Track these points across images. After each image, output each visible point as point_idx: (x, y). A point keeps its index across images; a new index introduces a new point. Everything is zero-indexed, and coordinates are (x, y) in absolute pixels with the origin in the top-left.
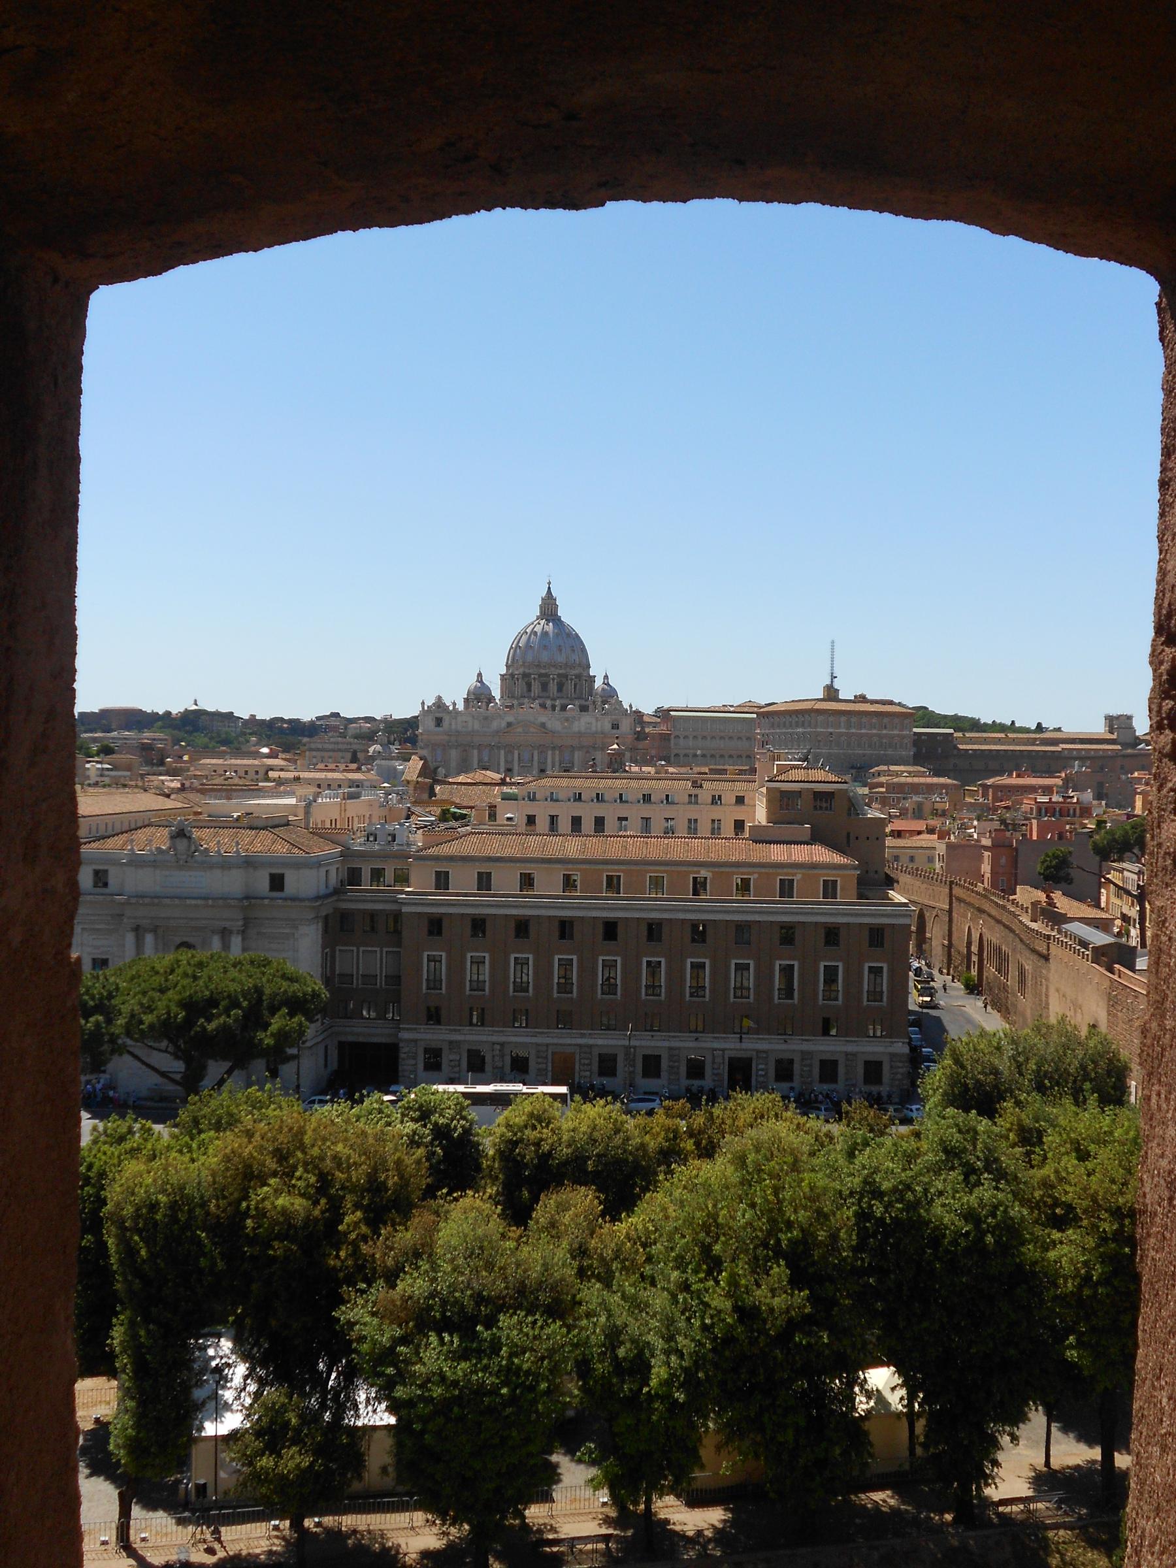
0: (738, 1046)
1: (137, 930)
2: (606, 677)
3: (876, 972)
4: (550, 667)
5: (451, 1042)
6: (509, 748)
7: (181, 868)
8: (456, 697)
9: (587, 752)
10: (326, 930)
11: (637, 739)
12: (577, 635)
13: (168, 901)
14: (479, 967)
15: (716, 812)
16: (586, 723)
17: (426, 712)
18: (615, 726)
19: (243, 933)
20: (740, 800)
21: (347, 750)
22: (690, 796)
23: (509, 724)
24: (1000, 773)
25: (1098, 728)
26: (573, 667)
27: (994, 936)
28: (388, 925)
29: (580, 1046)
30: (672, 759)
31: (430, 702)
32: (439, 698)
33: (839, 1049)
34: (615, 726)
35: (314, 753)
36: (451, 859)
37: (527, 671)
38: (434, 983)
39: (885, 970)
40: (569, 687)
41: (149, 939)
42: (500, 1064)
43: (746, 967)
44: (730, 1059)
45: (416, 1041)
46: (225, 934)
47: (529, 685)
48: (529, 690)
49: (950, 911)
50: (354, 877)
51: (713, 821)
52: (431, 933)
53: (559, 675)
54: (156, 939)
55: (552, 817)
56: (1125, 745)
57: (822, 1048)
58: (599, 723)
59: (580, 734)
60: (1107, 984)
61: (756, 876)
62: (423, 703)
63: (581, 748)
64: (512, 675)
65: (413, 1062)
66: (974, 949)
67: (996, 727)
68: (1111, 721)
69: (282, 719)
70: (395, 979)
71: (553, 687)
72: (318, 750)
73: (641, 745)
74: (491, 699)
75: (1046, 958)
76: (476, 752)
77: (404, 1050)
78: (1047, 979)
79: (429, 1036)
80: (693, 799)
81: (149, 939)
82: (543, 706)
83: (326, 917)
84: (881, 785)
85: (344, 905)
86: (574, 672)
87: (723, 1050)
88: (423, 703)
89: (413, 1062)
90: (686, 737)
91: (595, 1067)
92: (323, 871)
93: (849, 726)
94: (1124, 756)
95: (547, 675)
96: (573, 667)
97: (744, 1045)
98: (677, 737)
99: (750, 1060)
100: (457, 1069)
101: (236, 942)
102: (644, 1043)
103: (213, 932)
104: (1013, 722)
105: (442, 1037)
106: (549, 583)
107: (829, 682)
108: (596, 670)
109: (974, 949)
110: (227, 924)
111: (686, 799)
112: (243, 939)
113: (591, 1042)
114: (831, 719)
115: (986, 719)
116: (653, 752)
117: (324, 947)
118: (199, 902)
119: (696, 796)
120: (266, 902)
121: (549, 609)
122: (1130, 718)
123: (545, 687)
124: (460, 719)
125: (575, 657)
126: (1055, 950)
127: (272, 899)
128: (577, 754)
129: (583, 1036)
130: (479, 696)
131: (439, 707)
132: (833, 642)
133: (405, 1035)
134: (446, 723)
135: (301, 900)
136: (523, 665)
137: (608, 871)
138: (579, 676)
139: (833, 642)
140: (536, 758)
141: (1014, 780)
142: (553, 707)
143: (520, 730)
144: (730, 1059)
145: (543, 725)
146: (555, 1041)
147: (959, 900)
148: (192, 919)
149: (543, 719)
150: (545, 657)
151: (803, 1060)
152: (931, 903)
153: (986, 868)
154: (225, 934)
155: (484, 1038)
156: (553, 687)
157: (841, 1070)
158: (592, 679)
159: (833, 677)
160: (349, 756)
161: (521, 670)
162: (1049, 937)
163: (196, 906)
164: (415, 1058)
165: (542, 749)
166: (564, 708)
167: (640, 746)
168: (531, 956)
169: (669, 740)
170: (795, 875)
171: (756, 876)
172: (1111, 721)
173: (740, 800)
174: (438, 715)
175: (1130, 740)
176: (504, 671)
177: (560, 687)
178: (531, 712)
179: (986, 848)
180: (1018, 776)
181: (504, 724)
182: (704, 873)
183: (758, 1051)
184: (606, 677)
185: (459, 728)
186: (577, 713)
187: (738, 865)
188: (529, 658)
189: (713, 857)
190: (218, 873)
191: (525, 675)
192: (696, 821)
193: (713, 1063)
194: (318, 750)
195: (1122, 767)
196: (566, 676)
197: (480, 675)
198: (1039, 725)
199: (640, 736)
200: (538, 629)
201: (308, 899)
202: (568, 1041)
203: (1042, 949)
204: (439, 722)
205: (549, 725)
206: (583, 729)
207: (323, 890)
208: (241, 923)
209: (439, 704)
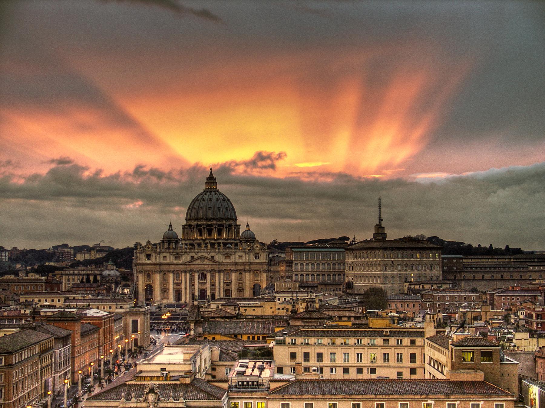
9: (240, 273)
11: (269, 264)
18: (257, 256)
20: (413, 342)
22: (384, 340)
23: (192, 257)
30: (294, 277)
37: (199, 223)
53: (219, 225)
58: (247, 256)
59: (236, 264)
63: (236, 271)
64: (190, 226)
76: (171, 275)
82: (212, 245)
95: (211, 225)
96: (226, 220)
104: (491, 245)
107: (378, 223)
115: (475, 245)
116: (282, 274)
119: (388, 340)
128: (233, 274)
132: (380, 199)
138: (230, 225)
139: (380, 199)
145: (213, 257)
149: (213, 254)
158: (238, 227)
159: (380, 220)
161: (196, 222)
169: (292, 266)
170: (480, 401)
171: (458, 402)
173: (413, 342)
174: (149, 253)
176: (184, 223)
181: (189, 258)
185: (162, 261)
191: (198, 225)
196: (222, 225)
197: (170, 226)
198: (507, 247)
200: (206, 197)
204: (149, 256)
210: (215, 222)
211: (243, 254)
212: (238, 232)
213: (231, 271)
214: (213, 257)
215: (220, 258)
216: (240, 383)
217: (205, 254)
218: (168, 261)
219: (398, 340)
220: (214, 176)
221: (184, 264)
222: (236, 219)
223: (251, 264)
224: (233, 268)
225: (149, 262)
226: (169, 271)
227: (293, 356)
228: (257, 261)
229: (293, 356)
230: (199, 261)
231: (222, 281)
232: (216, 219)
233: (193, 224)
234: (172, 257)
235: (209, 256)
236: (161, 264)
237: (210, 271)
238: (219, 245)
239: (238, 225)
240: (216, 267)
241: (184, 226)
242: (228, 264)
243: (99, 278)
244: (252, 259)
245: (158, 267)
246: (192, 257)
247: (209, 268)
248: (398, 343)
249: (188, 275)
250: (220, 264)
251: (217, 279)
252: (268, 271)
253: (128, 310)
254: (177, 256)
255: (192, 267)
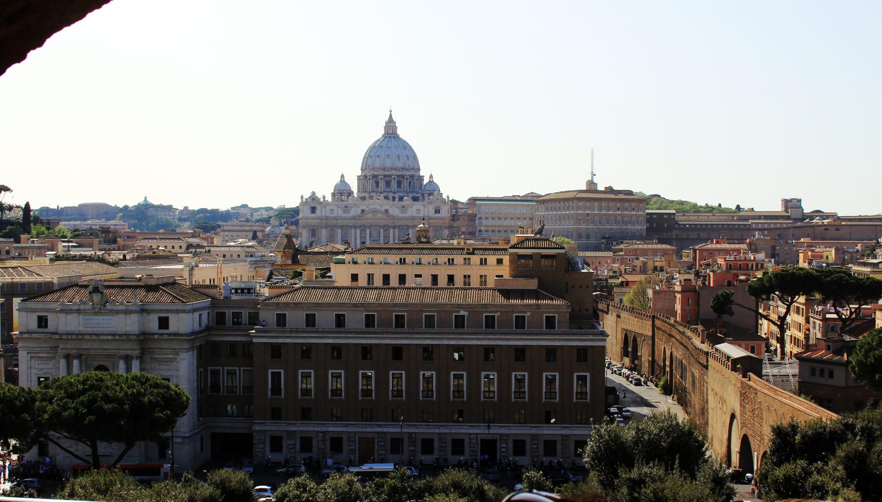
0: (487, 431)
1: (68, 358)
2: (431, 176)
3: (582, 379)
4: (393, 170)
5: (288, 432)
6: (363, 228)
7: (97, 314)
8: (325, 192)
10: (200, 357)
12: (411, 148)
13: (88, 337)
14: (307, 380)
15: (484, 270)
16: (416, 209)
17: (304, 203)
18: (437, 211)
19: (141, 358)
21: (250, 231)
23: (363, 211)
24: (705, 240)
25: (777, 207)
26: (407, 170)
27: (679, 354)
28: (244, 352)
29: (378, 433)
30: (477, 233)
31: (307, 195)
32: (314, 193)
33: (557, 432)
34: (437, 211)
35: (227, 233)
36: (287, 305)
38: (276, 390)
39: (588, 378)
40: (405, 184)
41: (76, 363)
42: (323, 447)
43: (461, 377)
44: (481, 440)
45: (264, 431)
46: (128, 359)
47: (377, 183)
48: (377, 186)
49: (653, 337)
50: (220, 318)
51: (481, 276)
52: (273, 356)
53: (398, 176)
54: (81, 363)
55: (369, 275)
56: (796, 220)
57: (545, 432)
60: (739, 385)
61: (499, 314)
62: (302, 197)
64: (365, 177)
65: (262, 446)
66: (668, 363)
67: (710, 209)
68: (787, 203)
69: (170, 208)
70: (249, 389)
71: (394, 184)
72: (229, 231)
73: (455, 224)
74: (350, 193)
75: (706, 367)
76: (339, 230)
77: (256, 437)
78: (707, 383)
79: (273, 428)
80: (467, 262)
81: (76, 363)
82: (386, 198)
83: (200, 346)
84: (621, 250)
85: (214, 338)
86: (409, 173)
87: (477, 434)
88: (302, 197)
89: (262, 446)
90: (487, 218)
91: (389, 447)
92: (197, 314)
93: (600, 209)
94: (794, 227)
95: (390, 176)
96: (407, 170)
97: (491, 431)
98: (480, 218)
99: (495, 441)
100: (293, 451)
101: (136, 364)
102: (421, 430)
103: (121, 358)
104: (720, 205)
105: (282, 428)
106: (391, 111)
107: (590, 179)
108: (425, 173)
109: (668, 363)
110: (129, 352)
111: (462, 261)
112: (141, 363)
113: (385, 430)
114: (588, 204)
116: (464, 230)
117: (198, 367)
118: (110, 337)
119: (469, 259)
120: (156, 337)
121: (391, 129)
122: (799, 201)
123: (388, 184)
124: (328, 208)
125: (410, 163)
126: (712, 362)
127: (161, 334)
129: (380, 426)
130: (342, 191)
131: (313, 199)
132: (592, 151)
133: (257, 428)
134: (318, 211)
135: (182, 335)
136: (373, 169)
137: (396, 311)
138: (412, 177)
139: (592, 151)
140: (382, 234)
141: (714, 246)
142: (394, 199)
143: (370, 215)
144: (481, 440)
145: (387, 211)
146: (360, 430)
147: (659, 329)
148: (105, 349)
150: (388, 164)
151: (532, 440)
152: (641, 331)
153: (678, 307)
154: (128, 359)
155: (311, 429)
156: (394, 184)
157: (559, 446)
158: (421, 178)
160: (251, 234)
161: (372, 172)
162: (707, 353)
163: (108, 340)
164: (264, 443)
165: (386, 228)
166: (401, 199)
167: (455, 225)
168: (343, 372)
170: (525, 312)
171: (499, 314)
172: (787, 203)
174: (313, 205)
175: (799, 216)
176: (359, 173)
177: (399, 184)
178: (379, 203)
179: (678, 292)
180: (717, 242)
181: (359, 212)
182: (462, 313)
183: (501, 435)
184: (431, 176)
185: (328, 215)
186: (410, 202)
187: (485, 306)
188: (377, 165)
189: (469, 301)
190: (122, 316)
191: (374, 176)
192: (469, 276)
193: (470, 443)
194: (229, 231)
195: (793, 235)
196: (403, 176)
197: (342, 176)
198: (738, 207)
199: (454, 218)
201: (186, 335)
202: (369, 430)
203: (704, 361)
204: (313, 210)
205: (390, 212)
206: (414, 214)
207: (197, 328)
208: (138, 352)
209: (313, 197)
210: (394, 172)
211: (421, 207)
212: (421, 184)
213: (408, 227)
214: (387, 211)
215: (394, 210)
216: (233, 291)
217: (378, 207)
218: (335, 215)
219: (481, 259)
220: (394, 119)
221: (354, 218)
222: (419, 170)
223: (430, 218)
224: (410, 223)
225: (313, 215)
226: (338, 227)
227: (355, 277)
228: (438, 215)
229: (355, 277)
230: (370, 215)
231: (397, 238)
232: (395, 169)
233: (368, 174)
234: (340, 210)
235: (383, 209)
236: (327, 218)
237: (384, 227)
238: (394, 199)
239: (420, 177)
240: (390, 222)
241: (358, 177)
242: (404, 219)
243: (259, 235)
244: (432, 213)
245: (324, 221)
246: (363, 211)
247: (383, 223)
248: (481, 263)
249: (358, 231)
250: (394, 218)
251: (391, 236)
252: (450, 227)
253: (259, 259)
254: (347, 208)
255: (363, 222)
